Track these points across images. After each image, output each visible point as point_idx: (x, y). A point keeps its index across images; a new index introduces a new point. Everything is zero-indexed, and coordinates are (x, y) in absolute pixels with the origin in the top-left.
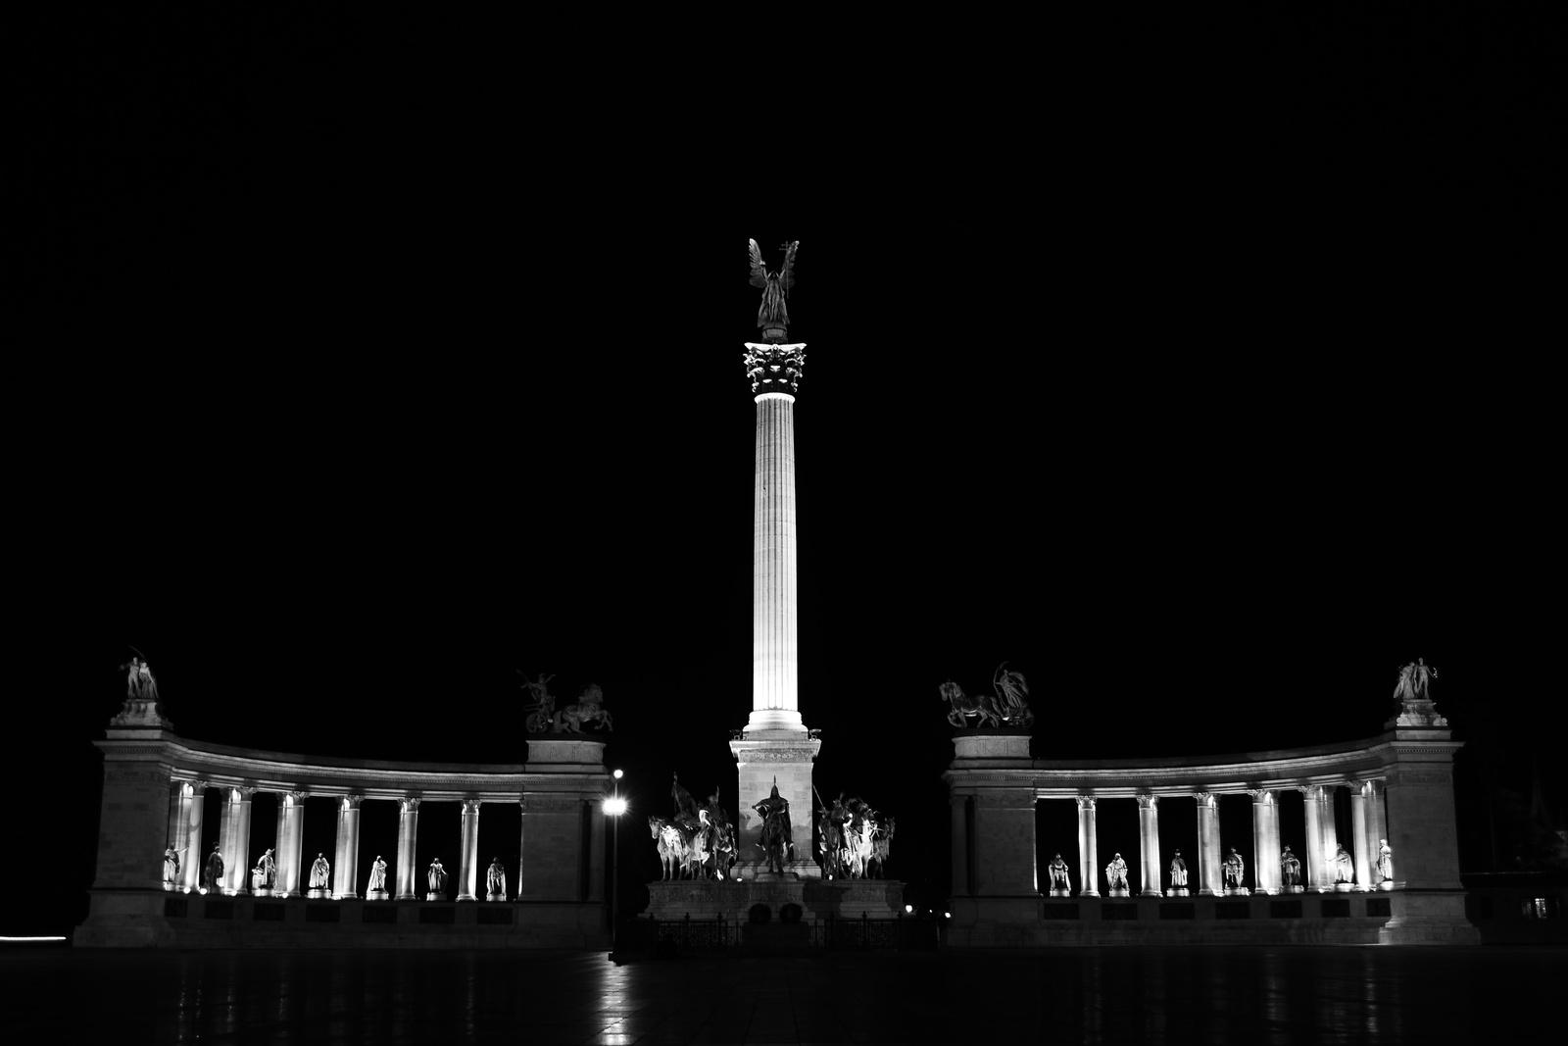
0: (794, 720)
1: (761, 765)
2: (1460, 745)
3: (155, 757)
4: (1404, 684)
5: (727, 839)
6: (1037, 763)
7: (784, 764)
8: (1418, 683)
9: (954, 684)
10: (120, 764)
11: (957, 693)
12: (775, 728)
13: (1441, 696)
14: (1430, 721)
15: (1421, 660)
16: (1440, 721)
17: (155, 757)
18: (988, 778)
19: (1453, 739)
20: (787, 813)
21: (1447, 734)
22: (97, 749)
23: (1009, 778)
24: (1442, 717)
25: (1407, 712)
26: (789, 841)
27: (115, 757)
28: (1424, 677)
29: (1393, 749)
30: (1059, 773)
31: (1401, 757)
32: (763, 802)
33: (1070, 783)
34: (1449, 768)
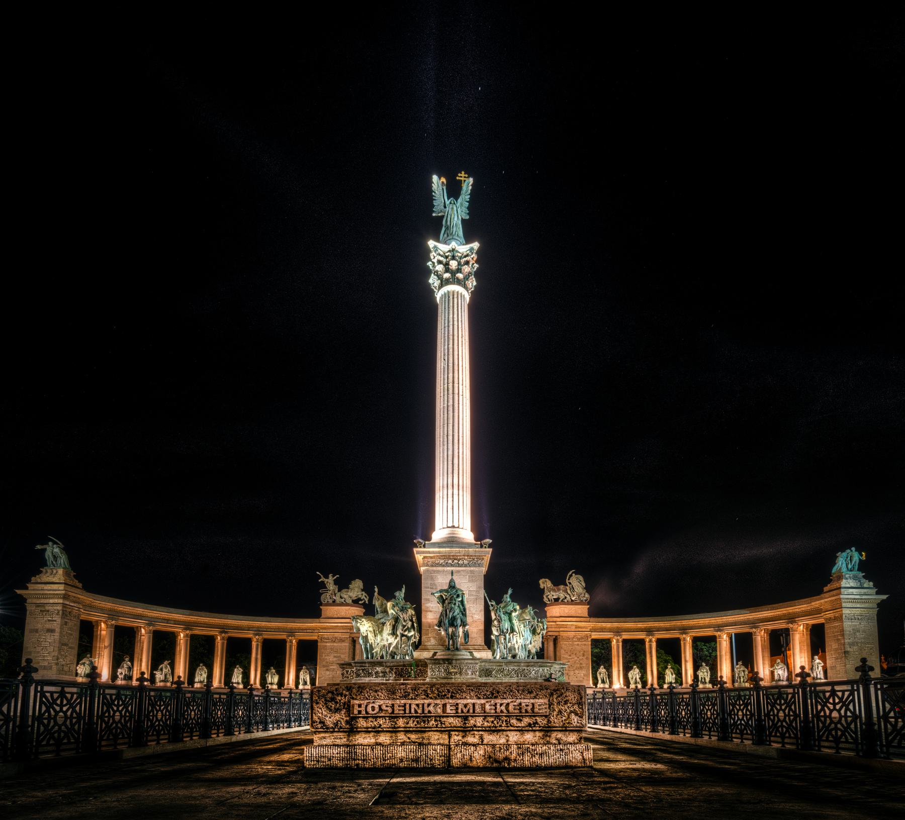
0: (467, 534)
1: (440, 569)
2: (885, 597)
3: (61, 601)
5: (409, 624)
6: (592, 619)
10: (38, 605)
12: (452, 541)
17: (61, 601)
18: (566, 626)
19: (877, 593)
20: (462, 602)
22: (21, 596)
23: (577, 627)
26: (464, 624)
27: (35, 601)
29: (840, 599)
30: (604, 625)
32: (441, 591)
33: (610, 630)
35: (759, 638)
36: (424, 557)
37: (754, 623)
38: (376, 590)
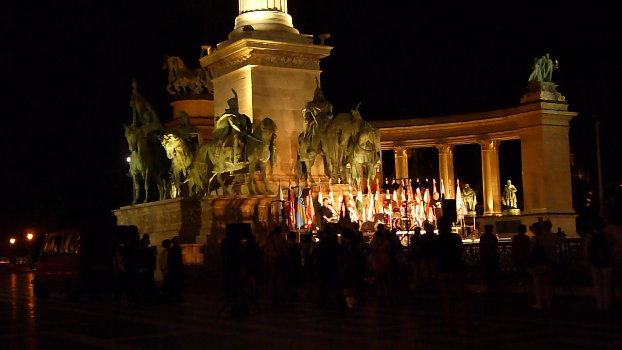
1: (272, 68)
2: (575, 114)
4: (537, 72)
7: (296, 70)
8: (546, 70)
9: (178, 58)
11: (181, 65)
13: (560, 80)
14: (557, 97)
15: (548, 55)
16: (562, 98)
19: (569, 110)
21: (566, 106)
24: (562, 95)
25: (543, 90)
28: (551, 67)
29: (541, 114)
31: (544, 121)
34: (567, 130)
35: (445, 156)
36: (254, 51)
37: (441, 137)
38: (134, 85)
